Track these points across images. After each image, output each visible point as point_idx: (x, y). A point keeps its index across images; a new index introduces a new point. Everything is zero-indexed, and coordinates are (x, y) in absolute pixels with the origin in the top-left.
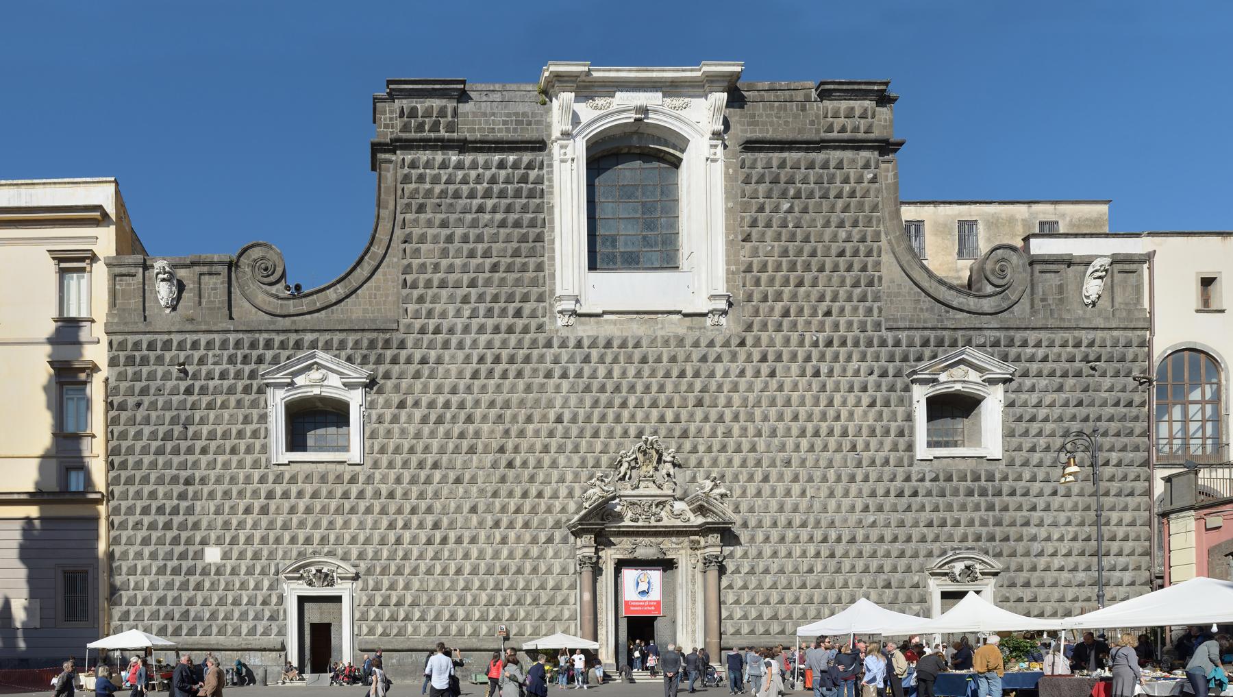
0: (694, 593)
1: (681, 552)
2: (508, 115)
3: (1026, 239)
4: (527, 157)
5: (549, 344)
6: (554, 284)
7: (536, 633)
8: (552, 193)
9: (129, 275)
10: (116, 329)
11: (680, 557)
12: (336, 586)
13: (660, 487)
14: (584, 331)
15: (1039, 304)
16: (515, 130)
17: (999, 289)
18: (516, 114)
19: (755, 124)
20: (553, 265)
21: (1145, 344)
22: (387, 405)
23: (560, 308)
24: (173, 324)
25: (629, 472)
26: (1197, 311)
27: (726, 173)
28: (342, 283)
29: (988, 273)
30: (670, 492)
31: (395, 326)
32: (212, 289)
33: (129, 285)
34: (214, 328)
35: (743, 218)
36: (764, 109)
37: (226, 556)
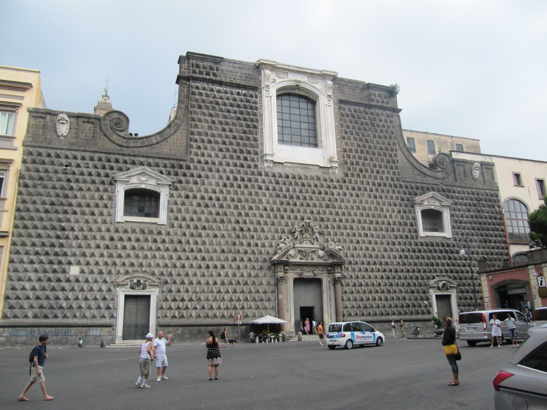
0: (330, 295)
2: (242, 74)
3: (451, 151)
4: (251, 92)
5: (260, 174)
7: (254, 316)
8: (262, 109)
9: (41, 117)
10: (29, 143)
12: (147, 290)
13: (313, 244)
15: (458, 177)
16: (245, 80)
17: (443, 170)
18: (246, 74)
19: (345, 94)
21: (497, 196)
22: (180, 196)
23: (265, 159)
24: (64, 145)
26: (515, 186)
27: (334, 111)
28: (159, 135)
29: (438, 163)
30: (317, 246)
31: (186, 158)
32: (88, 130)
33: (40, 122)
34: (88, 149)
35: (341, 130)
36: (348, 88)
37: (82, 271)
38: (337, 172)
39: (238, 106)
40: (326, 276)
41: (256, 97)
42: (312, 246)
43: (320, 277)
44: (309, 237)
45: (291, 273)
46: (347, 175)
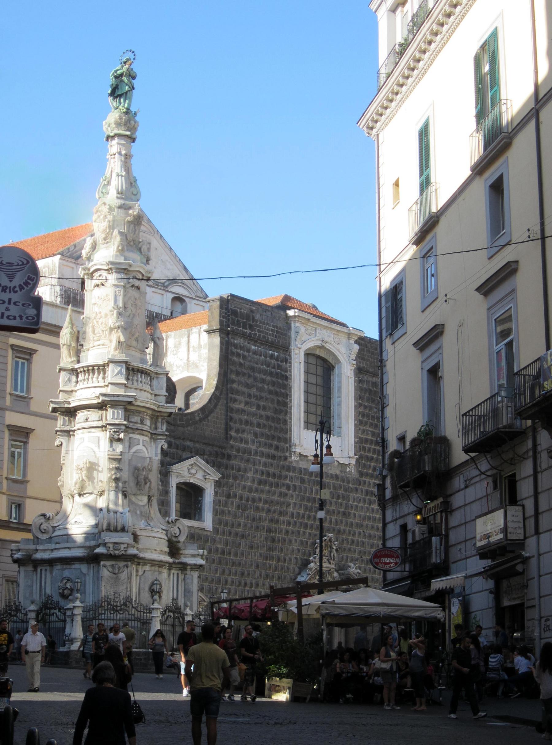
2: (273, 326)
6: (291, 434)
8: (291, 379)
13: (330, 563)
14: (302, 465)
18: (277, 327)
20: (291, 422)
23: (294, 450)
38: (353, 471)
39: (271, 374)
41: (286, 363)
46: (361, 474)
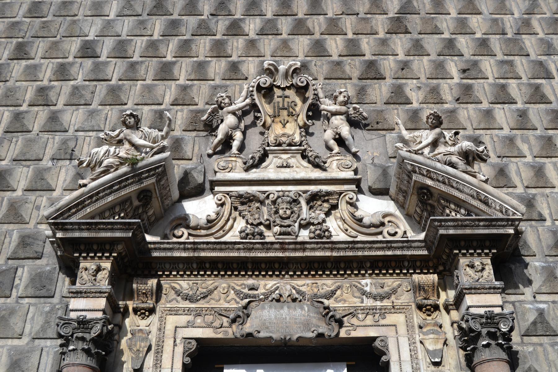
1: (391, 319)
11: (389, 333)
25: (238, 135)
40: (409, 326)
42: (317, 174)
43: (372, 333)
44: (297, 138)
45: (174, 312)
